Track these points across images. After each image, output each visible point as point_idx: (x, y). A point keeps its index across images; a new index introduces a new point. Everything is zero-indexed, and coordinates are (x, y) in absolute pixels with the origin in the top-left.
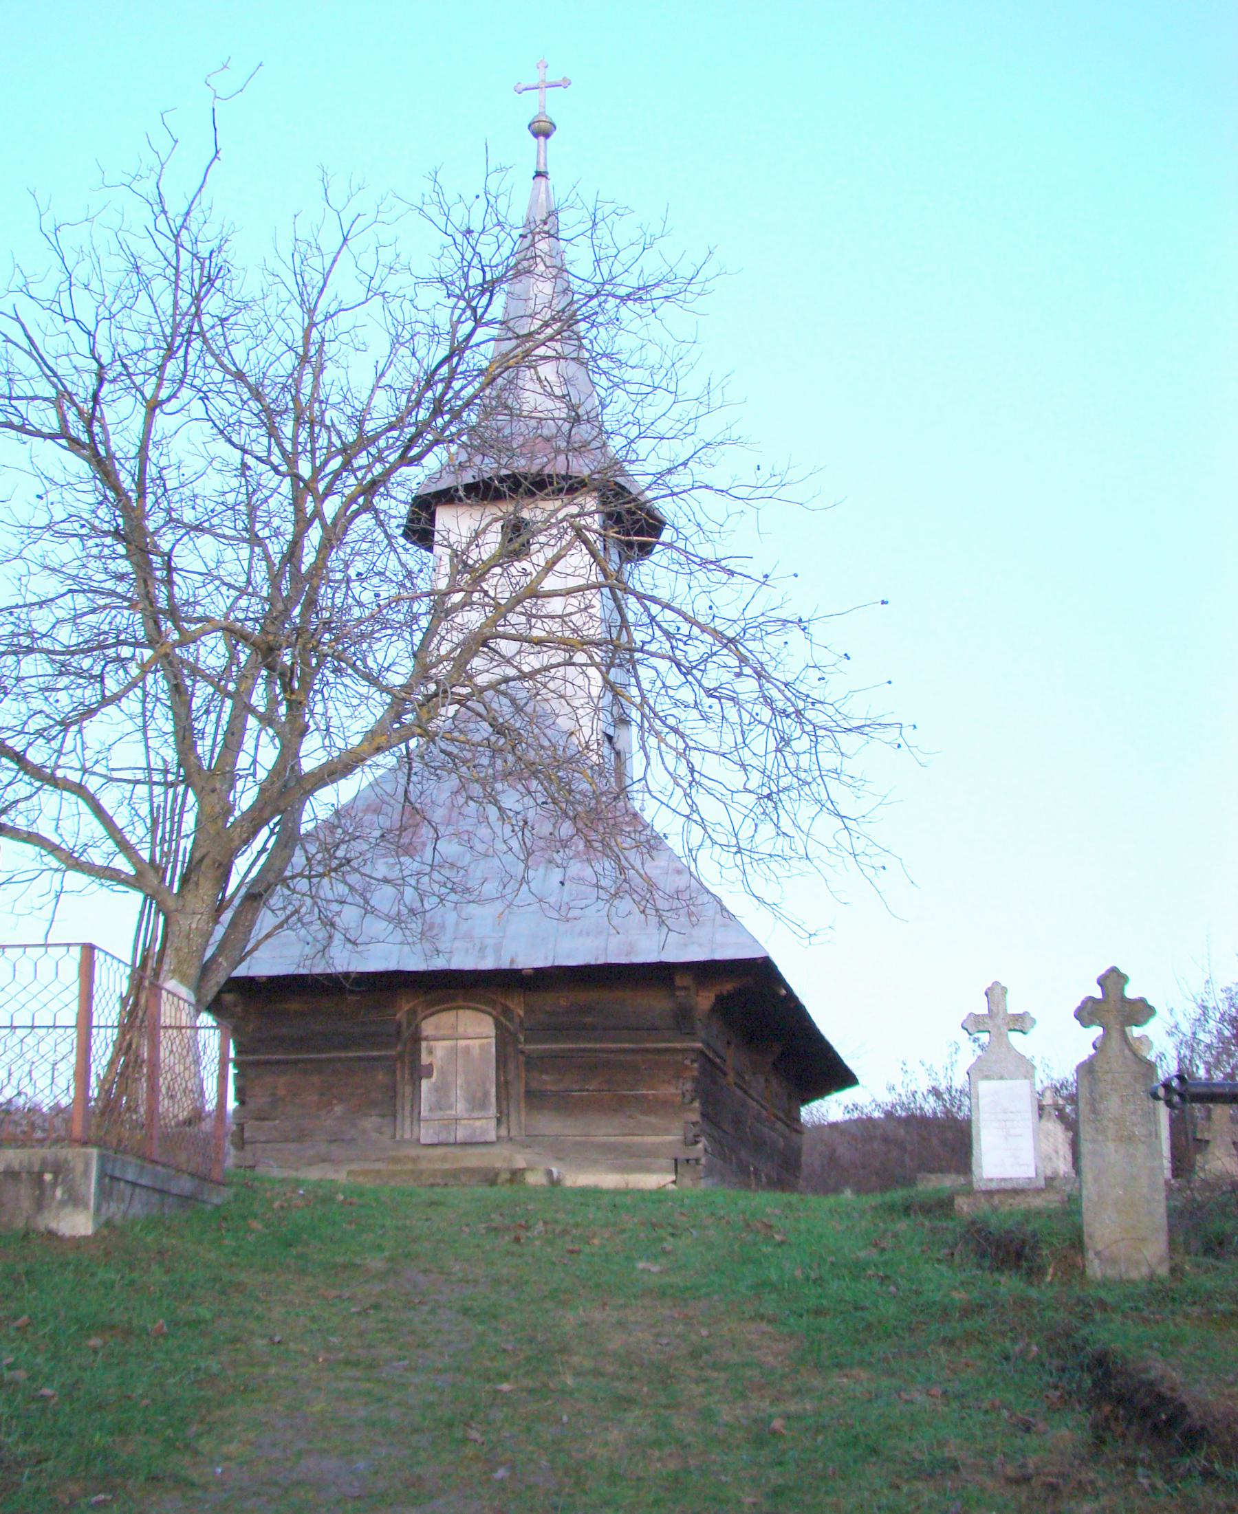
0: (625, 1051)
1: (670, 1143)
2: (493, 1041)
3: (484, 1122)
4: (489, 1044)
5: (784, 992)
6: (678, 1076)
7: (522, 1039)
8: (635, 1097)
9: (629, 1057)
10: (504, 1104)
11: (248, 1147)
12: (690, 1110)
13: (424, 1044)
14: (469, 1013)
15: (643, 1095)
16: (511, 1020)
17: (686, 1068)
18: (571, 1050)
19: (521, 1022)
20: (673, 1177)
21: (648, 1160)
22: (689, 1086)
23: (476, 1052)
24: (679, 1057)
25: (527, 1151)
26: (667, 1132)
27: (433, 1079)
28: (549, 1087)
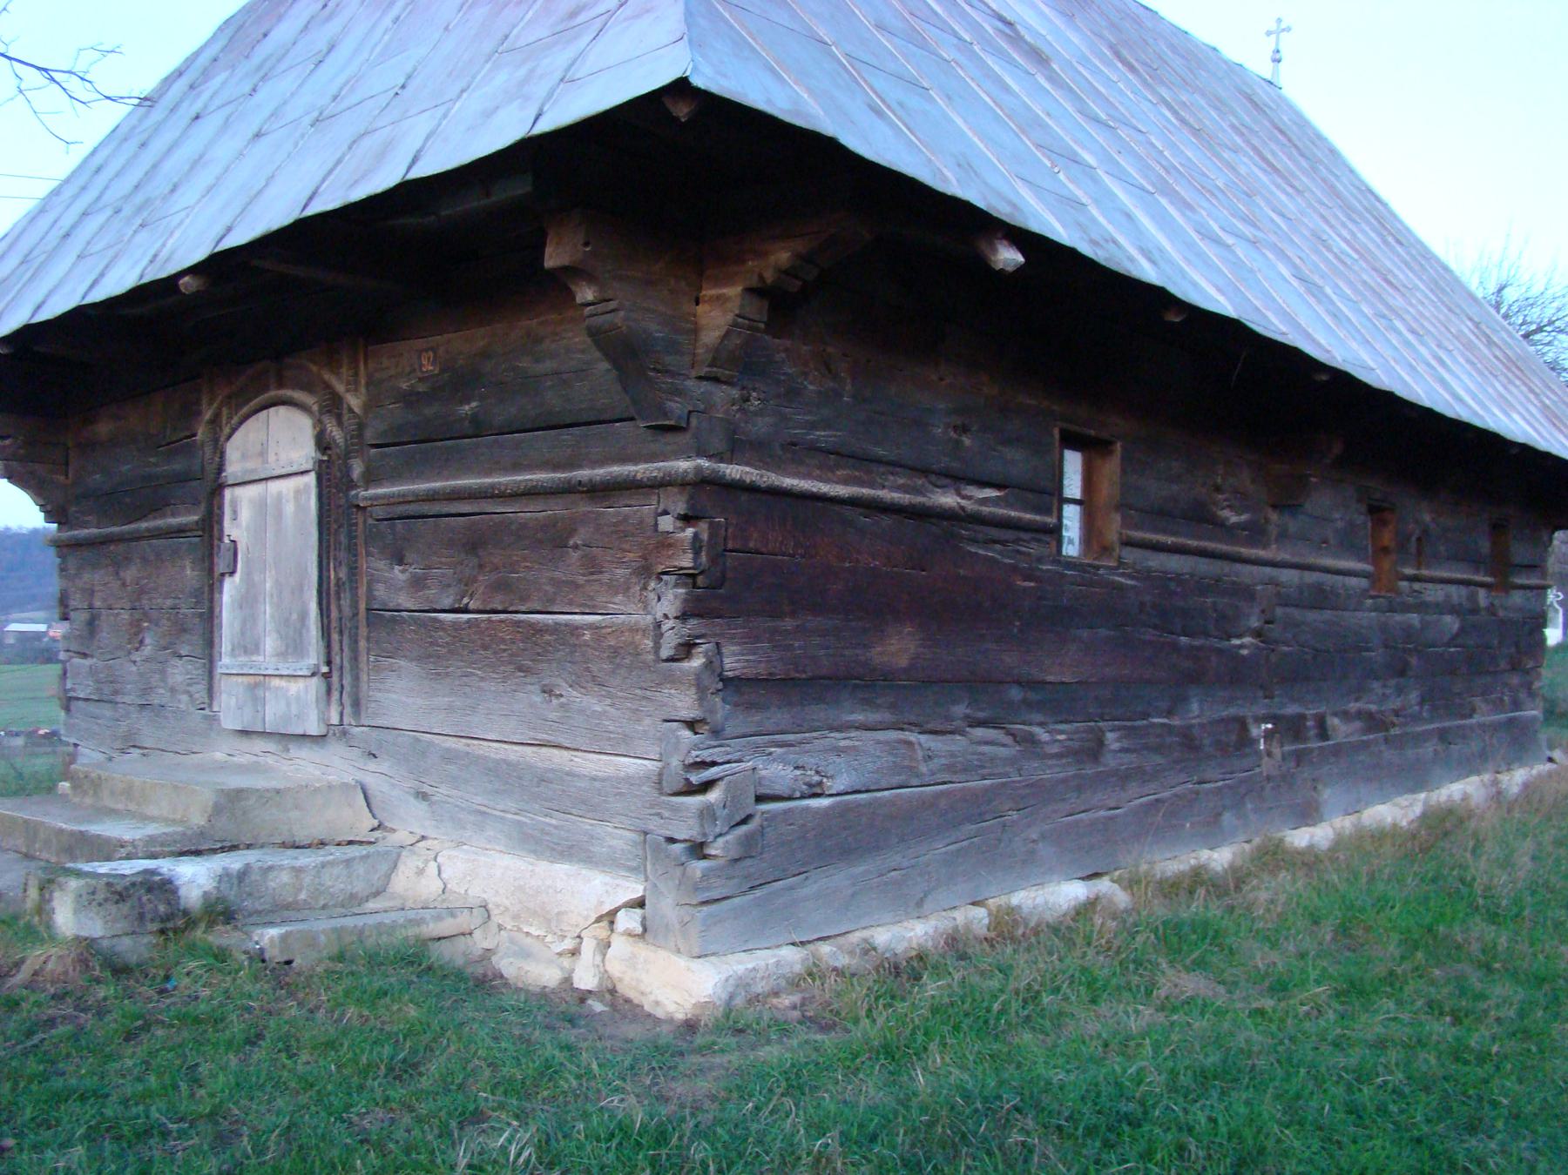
0: (532, 493)
1: (628, 780)
2: (311, 479)
3: (301, 684)
4: (307, 486)
5: (1008, 257)
6: (645, 572)
7: (357, 469)
8: (555, 629)
9: (555, 509)
10: (335, 637)
11: (75, 705)
12: (671, 680)
13: (228, 493)
14: (282, 410)
15: (575, 629)
16: (339, 419)
17: (665, 543)
18: (432, 497)
19: (361, 427)
20: (634, 889)
21: (587, 824)
22: (668, 601)
23: (289, 509)
24: (644, 509)
25: (372, 765)
26: (621, 745)
27: (237, 577)
28: (404, 600)
